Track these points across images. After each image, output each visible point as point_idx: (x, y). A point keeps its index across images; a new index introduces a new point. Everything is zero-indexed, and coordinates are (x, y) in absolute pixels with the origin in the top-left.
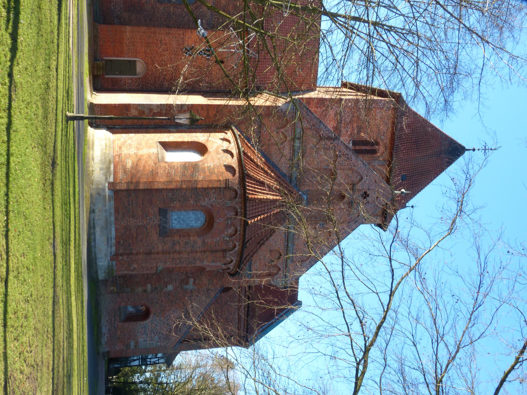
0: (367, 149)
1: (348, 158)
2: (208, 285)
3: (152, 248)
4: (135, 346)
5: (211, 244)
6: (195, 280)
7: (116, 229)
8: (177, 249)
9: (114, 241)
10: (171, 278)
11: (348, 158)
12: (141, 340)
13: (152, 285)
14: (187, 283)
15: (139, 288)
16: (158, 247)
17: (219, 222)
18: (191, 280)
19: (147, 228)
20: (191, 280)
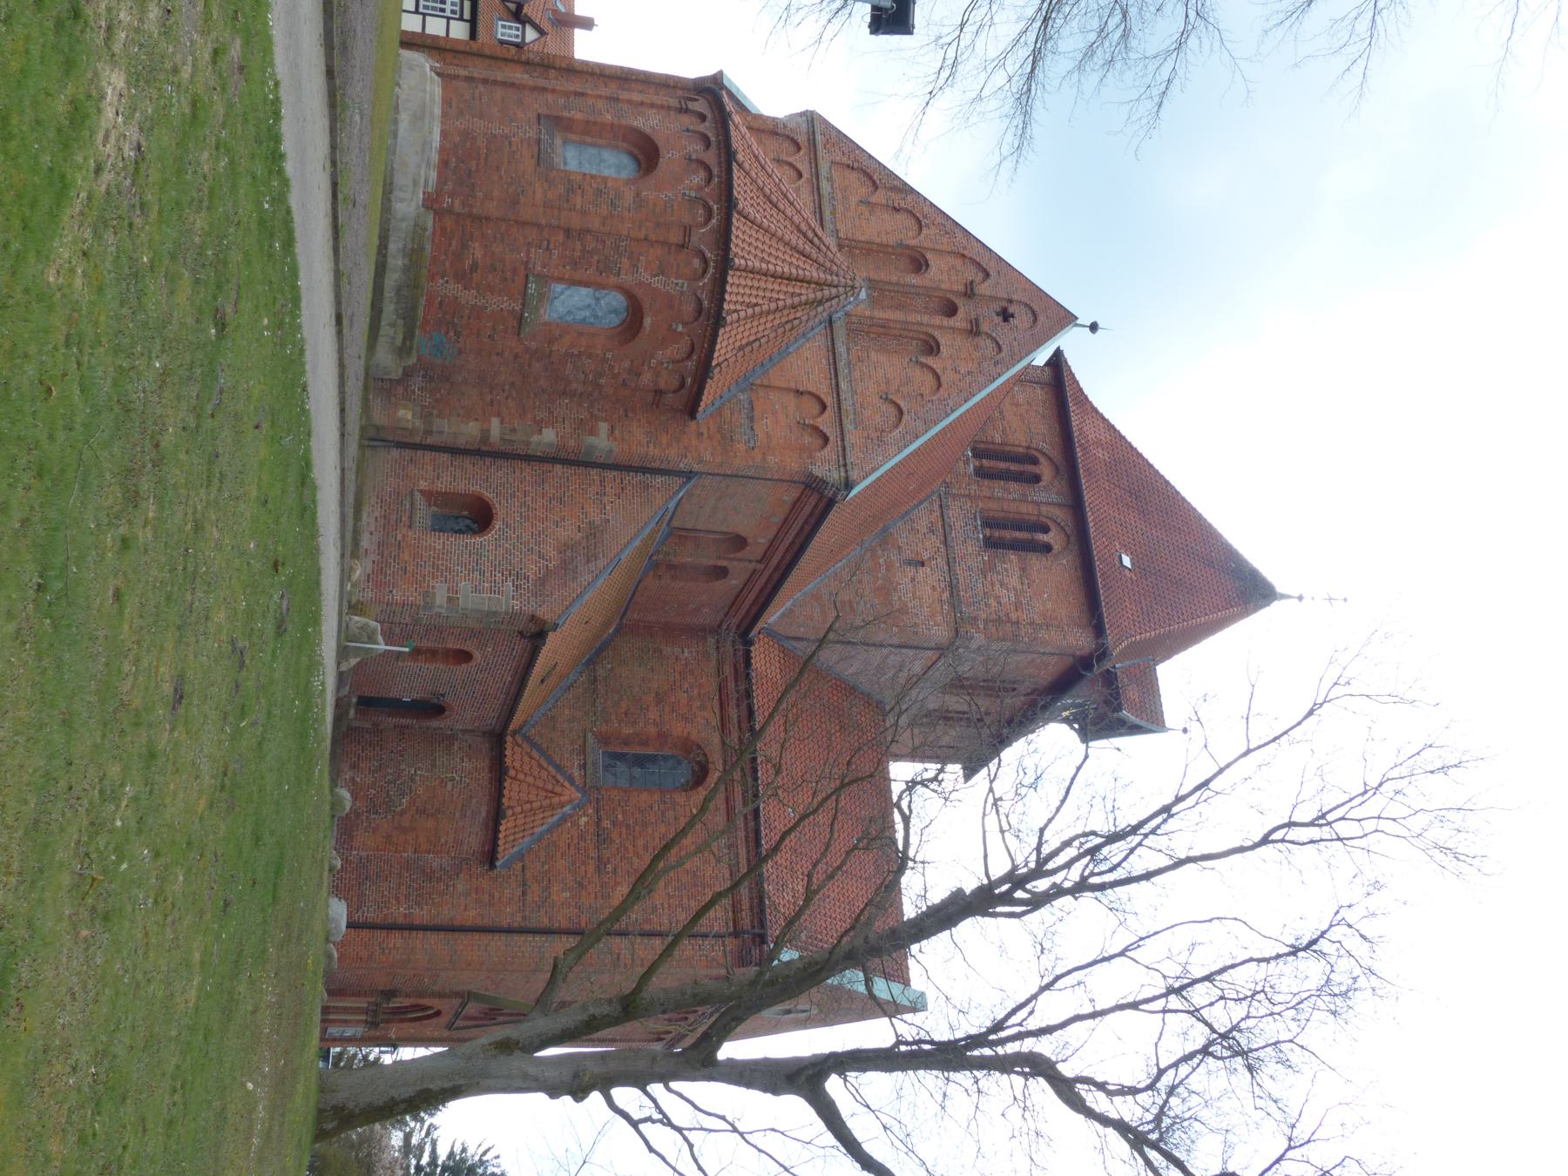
0: (1012, 468)
1: (947, 233)
2: (648, 447)
3: (519, 190)
4: (450, 600)
5: (655, 205)
6: (612, 428)
7: (444, 134)
8: (578, 207)
9: (435, 157)
10: (551, 413)
11: (947, 233)
12: (464, 585)
13: (502, 423)
14: (593, 432)
15: (471, 424)
16: (534, 192)
17: (670, 158)
18: (603, 427)
19: (510, 143)
20: (603, 427)
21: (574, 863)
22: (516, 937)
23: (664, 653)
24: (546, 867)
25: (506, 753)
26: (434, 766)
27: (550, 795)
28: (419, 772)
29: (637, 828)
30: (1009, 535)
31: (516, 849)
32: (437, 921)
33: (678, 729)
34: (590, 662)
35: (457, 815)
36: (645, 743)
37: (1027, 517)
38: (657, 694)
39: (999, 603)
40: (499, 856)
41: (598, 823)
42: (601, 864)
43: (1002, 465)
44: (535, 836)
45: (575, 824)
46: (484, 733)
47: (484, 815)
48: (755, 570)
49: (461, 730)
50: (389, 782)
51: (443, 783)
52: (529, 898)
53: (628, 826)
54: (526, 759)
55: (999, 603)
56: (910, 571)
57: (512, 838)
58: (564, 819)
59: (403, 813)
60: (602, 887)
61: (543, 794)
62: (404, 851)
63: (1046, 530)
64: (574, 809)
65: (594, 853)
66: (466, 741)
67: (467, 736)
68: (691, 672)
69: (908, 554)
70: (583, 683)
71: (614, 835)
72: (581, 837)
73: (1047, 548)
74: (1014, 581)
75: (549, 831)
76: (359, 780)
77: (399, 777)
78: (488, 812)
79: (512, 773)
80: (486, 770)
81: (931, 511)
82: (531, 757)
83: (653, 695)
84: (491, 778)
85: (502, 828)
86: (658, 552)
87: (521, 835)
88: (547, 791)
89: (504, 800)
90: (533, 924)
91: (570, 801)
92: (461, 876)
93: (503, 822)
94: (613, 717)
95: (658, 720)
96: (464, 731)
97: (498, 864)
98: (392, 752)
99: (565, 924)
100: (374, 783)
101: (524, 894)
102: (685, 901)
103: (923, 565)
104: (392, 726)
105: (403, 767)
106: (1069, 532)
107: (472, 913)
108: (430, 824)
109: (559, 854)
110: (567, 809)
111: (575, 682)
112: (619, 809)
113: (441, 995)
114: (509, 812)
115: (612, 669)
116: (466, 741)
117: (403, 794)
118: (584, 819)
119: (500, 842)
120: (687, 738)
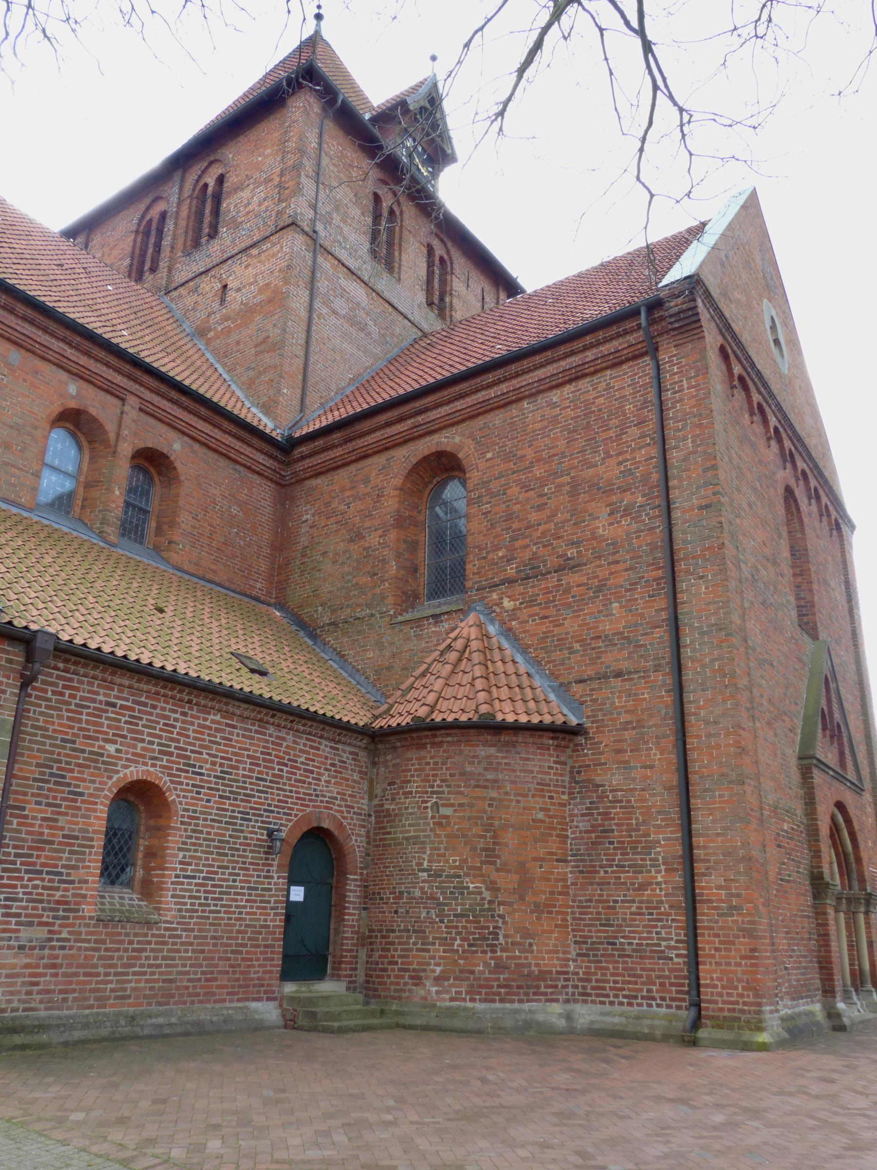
21: (568, 606)
22: (688, 675)
23: (306, 544)
24: (577, 646)
25: (394, 725)
26: (415, 840)
27: (466, 655)
28: (425, 864)
29: (515, 525)
30: (207, 219)
31: (552, 697)
32: (675, 813)
33: (391, 504)
34: (313, 636)
35: (494, 794)
36: (413, 546)
37: (193, 209)
38: (351, 540)
39: (265, 200)
40: (559, 720)
41: (511, 581)
42: (567, 566)
43: (150, 251)
44: (532, 671)
45: (513, 614)
46: (374, 764)
47: (492, 751)
48: (141, 409)
49: (370, 800)
50: (441, 915)
51: (441, 823)
52: (625, 665)
53: (513, 539)
54: (413, 694)
55: (265, 200)
56: (231, 295)
57: (532, 704)
58: (508, 632)
59: (493, 888)
60: (599, 558)
61: (463, 665)
62: (566, 880)
63: (206, 186)
64: (492, 621)
65: (552, 580)
66: (385, 790)
67: (378, 791)
68: (328, 504)
69: (216, 305)
70: (336, 639)
71: (527, 555)
72: (531, 602)
73: (221, 180)
74: (245, 194)
75: (524, 650)
76: (438, 969)
77: (433, 898)
78: (486, 743)
79: (422, 712)
80: (422, 753)
81: (180, 296)
82: (411, 687)
83: (352, 547)
84: (433, 744)
85: (510, 718)
86: (101, 534)
87: (528, 691)
88: (460, 660)
89: (464, 718)
90: (666, 654)
91: (480, 626)
92: (598, 780)
93: (499, 717)
94: (377, 591)
95: (380, 532)
96: (371, 796)
97: (574, 721)
98: (396, 912)
99: (662, 602)
100: (444, 941)
101: (618, 674)
102: (612, 433)
103: (225, 286)
104: (364, 913)
105: (417, 893)
106: (206, 164)
107: (656, 755)
108: (510, 839)
109: (557, 631)
110: (492, 630)
111: (335, 649)
112: (490, 556)
113: (810, 801)
114: (484, 709)
115: (323, 605)
116: (385, 790)
117: (462, 889)
118: (507, 604)
119: (535, 719)
120: (401, 489)
